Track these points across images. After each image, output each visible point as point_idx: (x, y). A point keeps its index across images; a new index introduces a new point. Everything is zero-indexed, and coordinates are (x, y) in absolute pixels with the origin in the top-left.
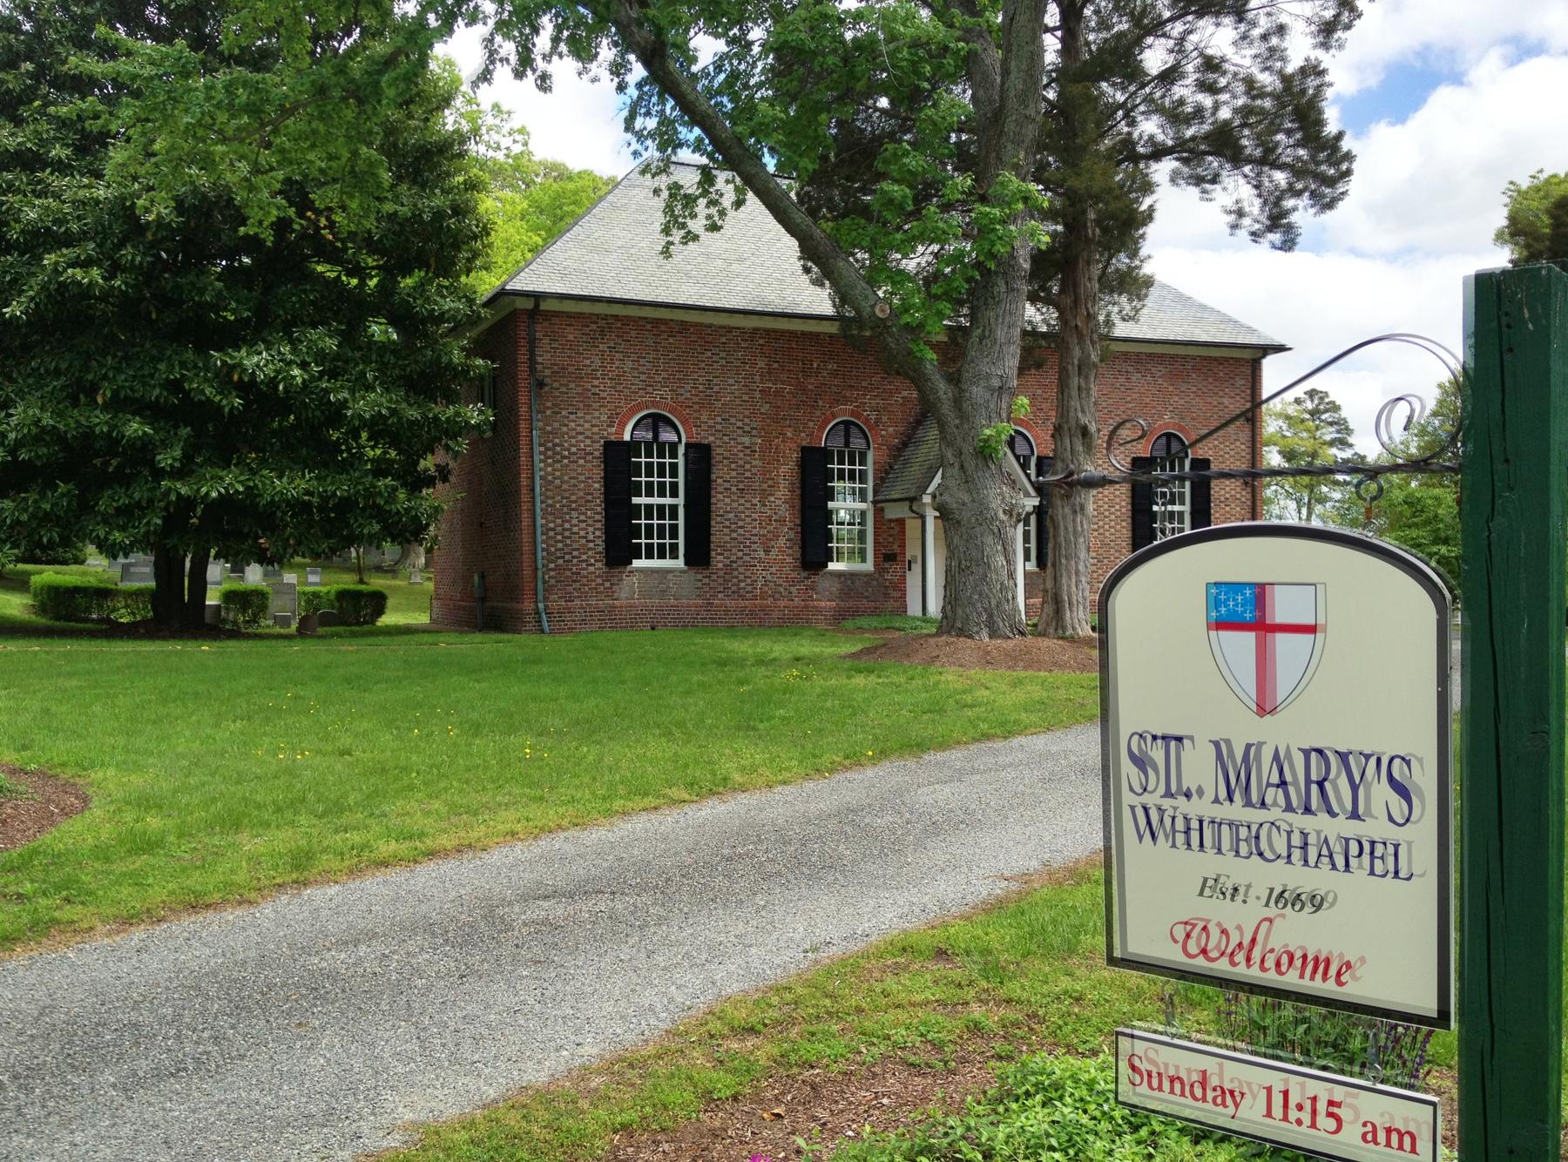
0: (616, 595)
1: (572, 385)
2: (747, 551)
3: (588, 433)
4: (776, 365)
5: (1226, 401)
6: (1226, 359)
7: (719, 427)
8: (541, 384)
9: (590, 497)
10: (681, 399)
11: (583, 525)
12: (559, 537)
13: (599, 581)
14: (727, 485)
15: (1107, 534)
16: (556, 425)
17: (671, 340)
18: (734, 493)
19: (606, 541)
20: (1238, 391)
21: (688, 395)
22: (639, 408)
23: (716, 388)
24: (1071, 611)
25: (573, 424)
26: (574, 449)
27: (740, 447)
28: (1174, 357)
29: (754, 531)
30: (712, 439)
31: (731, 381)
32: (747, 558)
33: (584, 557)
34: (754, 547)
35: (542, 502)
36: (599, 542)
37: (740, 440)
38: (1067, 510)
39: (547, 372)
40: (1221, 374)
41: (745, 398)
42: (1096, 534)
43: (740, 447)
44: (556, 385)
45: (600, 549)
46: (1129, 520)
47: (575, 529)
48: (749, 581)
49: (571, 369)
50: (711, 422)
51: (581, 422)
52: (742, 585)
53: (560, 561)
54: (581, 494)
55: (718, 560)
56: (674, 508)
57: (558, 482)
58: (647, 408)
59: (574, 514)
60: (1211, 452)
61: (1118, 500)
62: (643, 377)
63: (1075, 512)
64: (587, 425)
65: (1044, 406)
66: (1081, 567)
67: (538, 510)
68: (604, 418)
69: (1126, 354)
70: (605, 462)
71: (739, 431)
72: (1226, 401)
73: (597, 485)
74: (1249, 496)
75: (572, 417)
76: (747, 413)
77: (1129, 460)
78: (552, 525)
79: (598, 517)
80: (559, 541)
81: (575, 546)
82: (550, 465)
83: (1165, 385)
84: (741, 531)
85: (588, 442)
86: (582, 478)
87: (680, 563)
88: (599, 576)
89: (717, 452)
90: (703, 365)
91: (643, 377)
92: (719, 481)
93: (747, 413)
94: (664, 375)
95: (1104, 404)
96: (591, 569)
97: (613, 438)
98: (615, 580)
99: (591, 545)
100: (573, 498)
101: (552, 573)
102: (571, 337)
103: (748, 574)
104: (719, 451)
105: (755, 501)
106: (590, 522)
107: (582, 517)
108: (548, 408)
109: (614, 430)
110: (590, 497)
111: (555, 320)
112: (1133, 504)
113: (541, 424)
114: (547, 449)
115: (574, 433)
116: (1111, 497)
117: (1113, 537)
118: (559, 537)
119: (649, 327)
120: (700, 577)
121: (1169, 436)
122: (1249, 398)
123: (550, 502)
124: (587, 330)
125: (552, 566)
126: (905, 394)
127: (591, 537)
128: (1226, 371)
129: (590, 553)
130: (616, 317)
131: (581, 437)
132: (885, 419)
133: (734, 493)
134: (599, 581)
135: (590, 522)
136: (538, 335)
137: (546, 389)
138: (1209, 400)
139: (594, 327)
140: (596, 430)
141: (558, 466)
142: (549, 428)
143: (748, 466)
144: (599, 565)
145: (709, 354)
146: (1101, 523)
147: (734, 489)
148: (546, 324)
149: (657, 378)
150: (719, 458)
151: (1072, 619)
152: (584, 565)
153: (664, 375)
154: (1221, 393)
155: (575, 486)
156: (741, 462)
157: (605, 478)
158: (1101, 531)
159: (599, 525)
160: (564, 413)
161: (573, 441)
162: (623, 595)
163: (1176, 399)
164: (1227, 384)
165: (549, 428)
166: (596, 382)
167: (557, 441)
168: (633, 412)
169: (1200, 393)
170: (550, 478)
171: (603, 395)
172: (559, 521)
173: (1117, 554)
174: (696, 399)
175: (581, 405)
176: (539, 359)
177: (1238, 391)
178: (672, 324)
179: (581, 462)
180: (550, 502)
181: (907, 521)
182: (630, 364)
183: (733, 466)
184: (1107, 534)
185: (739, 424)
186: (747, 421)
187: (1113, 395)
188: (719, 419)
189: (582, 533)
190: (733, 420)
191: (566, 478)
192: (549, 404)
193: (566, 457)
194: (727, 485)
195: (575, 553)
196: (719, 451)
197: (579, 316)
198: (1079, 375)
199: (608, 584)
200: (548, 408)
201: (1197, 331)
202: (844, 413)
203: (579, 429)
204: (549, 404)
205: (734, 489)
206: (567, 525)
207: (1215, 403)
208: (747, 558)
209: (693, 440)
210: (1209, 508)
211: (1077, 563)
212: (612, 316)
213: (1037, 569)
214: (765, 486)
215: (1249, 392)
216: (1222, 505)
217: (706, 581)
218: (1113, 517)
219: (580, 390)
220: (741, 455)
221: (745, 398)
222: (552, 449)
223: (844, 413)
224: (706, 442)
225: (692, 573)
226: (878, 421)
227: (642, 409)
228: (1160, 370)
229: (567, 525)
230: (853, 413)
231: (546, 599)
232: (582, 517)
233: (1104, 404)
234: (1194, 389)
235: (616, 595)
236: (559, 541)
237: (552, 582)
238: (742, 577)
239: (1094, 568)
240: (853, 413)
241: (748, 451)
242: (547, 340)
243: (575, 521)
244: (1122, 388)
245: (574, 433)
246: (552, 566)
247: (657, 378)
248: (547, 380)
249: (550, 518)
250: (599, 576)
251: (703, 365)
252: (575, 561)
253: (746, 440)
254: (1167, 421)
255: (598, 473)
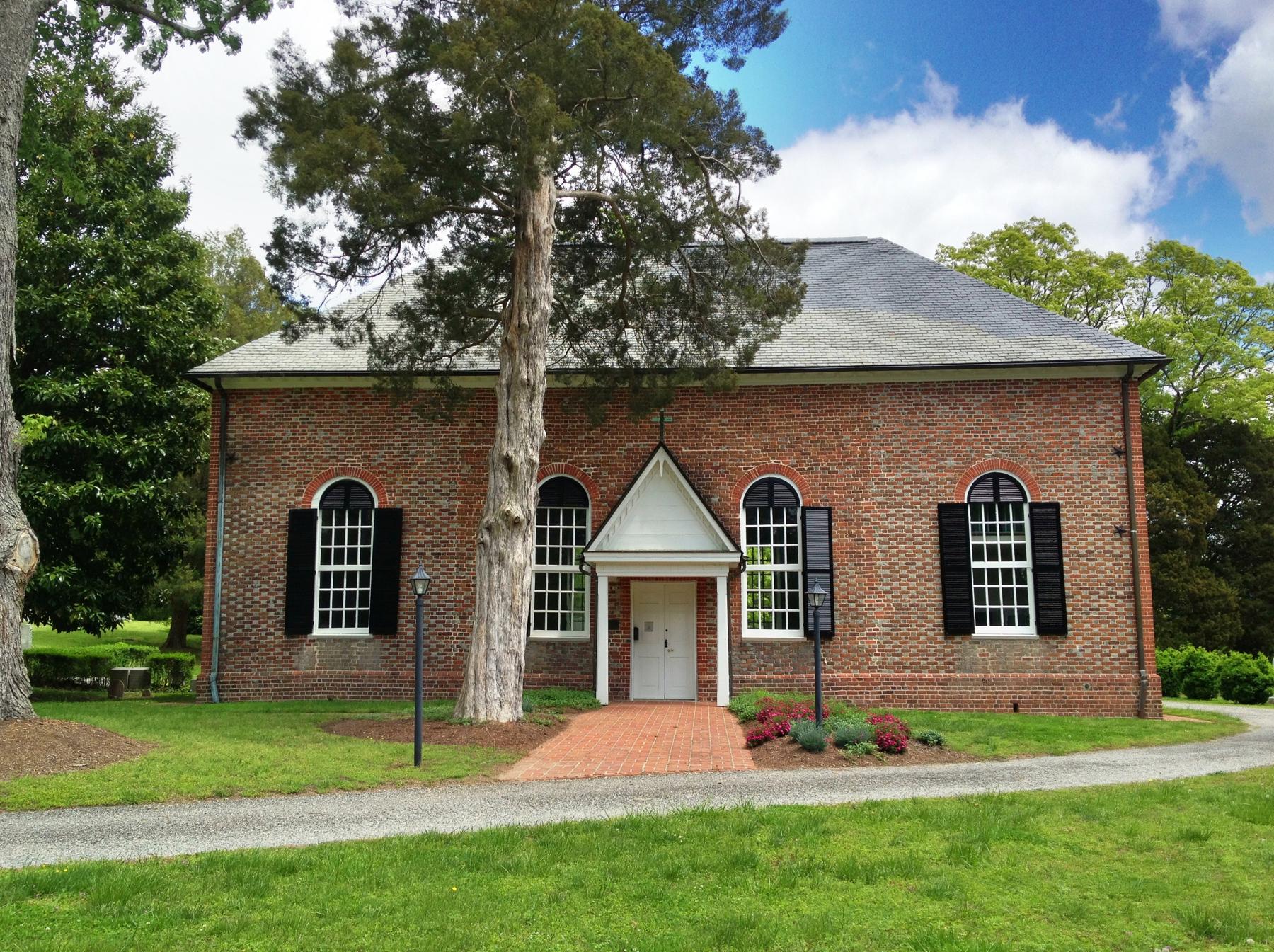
0: (294, 665)
1: (262, 458)
2: (440, 618)
3: (275, 503)
4: (479, 425)
5: (1082, 431)
6: (1081, 381)
7: (414, 491)
8: (231, 459)
9: (273, 566)
10: (375, 464)
11: (264, 594)
12: (240, 607)
13: (278, 650)
14: (421, 550)
15: (906, 597)
16: (244, 496)
17: (366, 408)
18: (428, 558)
19: (286, 610)
20: (1100, 418)
21: (382, 460)
22: (329, 476)
23: (412, 452)
24: (476, 689)
25: (260, 496)
26: (260, 520)
27: (437, 510)
28: (998, 384)
29: (449, 598)
30: (406, 503)
31: (429, 444)
32: (440, 626)
33: (264, 626)
34: (449, 613)
35: (223, 572)
36: (281, 611)
37: (437, 502)
38: (484, 561)
39: (238, 447)
40: (1073, 399)
41: (444, 459)
42: (889, 596)
43: (437, 510)
44: (246, 459)
45: (281, 617)
46: (938, 580)
47: (257, 598)
48: (441, 650)
49: (262, 442)
50: (406, 487)
51: (269, 492)
52: (434, 654)
53: (240, 631)
54: (264, 563)
55: (407, 628)
57: (242, 552)
58: (338, 475)
59: (257, 583)
60: (1061, 495)
61: (920, 556)
62: (335, 446)
63: (490, 563)
64: (274, 496)
65: (811, 450)
66: (493, 633)
67: (219, 580)
68: (292, 487)
69: (926, 384)
70: (290, 531)
71: (437, 495)
72: (1082, 431)
73: (281, 554)
74: (1126, 548)
75: (261, 488)
76: (446, 475)
77: (934, 507)
78: (233, 595)
79: (280, 586)
80: (240, 611)
81: (255, 614)
82: (235, 536)
83: (986, 416)
84: (435, 597)
85: (275, 511)
86: (266, 547)
88: (279, 646)
89: (411, 517)
90: (399, 430)
91: (335, 446)
92: (413, 546)
93: (446, 475)
94: (357, 442)
95: (896, 444)
96: (270, 638)
97: (300, 507)
98: (294, 650)
99: (272, 614)
100: (257, 567)
101: (231, 643)
102: (264, 412)
103: (441, 642)
104: (414, 515)
105: (452, 566)
106: (272, 590)
107: (265, 586)
108: (237, 481)
109: (301, 499)
110: (273, 566)
111: (249, 397)
112: (942, 560)
113: (229, 497)
114: (234, 520)
115: (261, 504)
116: (910, 552)
117: (914, 601)
118: (240, 607)
119: (343, 396)
120: (387, 645)
121: (996, 478)
122: (1119, 426)
123: (233, 571)
124: (280, 405)
125: (231, 635)
126: (631, 445)
127: (272, 606)
128: (1080, 395)
129: (270, 622)
130: (311, 390)
131: (267, 508)
132: (605, 473)
133: (428, 558)
134: (278, 650)
135: (272, 590)
136: (232, 413)
137: (237, 462)
138: (1058, 431)
139: (288, 400)
140: (283, 499)
141: (243, 536)
142: (236, 500)
143: (445, 530)
144: (279, 634)
145: (407, 418)
146: (895, 584)
147: (428, 553)
148: (240, 402)
149: (350, 446)
150: (414, 522)
151: (475, 698)
152: (263, 634)
153: (357, 442)
154: (1074, 422)
155: (258, 555)
156: (437, 526)
157: (289, 547)
158: (896, 593)
159: (281, 594)
160: (252, 484)
161: (260, 511)
162: (303, 665)
163: (1004, 432)
164: (1081, 411)
165: (236, 500)
166: (286, 453)
167: (244, 512)
168: (322, 480)
169: (1040, 423)
170: (234, 548)
171: (292, 465)
172: (241, 591)
173: (921, 621)
174: (390, 464)
175: (270, 476)
176: (232, 435)
177: (1100, 418)
178: (369, 392)
179: (267, 531)
180: (233, 571)
181: (633, 583)
182: (322, 434)
183: (428, 530)
184: (906, 597)
185: (437, 487)
186: (445, 483)
187: (909, 433)
188: (415, 483)
189: (263, 602)
190: (430, 483)
191: (250, 548)
192: (238, 477)
193: (251, 528)
194: (421, 550)
195: (255, 622)
196: (414, 515)
197: (273, 392)
198: (508, 398)
199: (287, 654)
200: (237, 481)
201: (1029, 351)
202: (557, 469)
203: (267, 499)
204: (238, 477)
205: (428, 553)
206: (248, 594)
207: (1065, 435)
208: (440, 626)
209: (385, 506)
210: (1061, 564)
211: (488, 627)
212: (307, 389)
213: (805, 639)
214: (463, 550)
215: (1118, 418)
216: (1084, 560)
217: (393, 650)
218: (913, 576)
219: (269, 462)
220: (438, 518)
221: (444, 459)
222: (239, 520)
223: (557, 469)
224: (399, 506)
225: (378, 642)
226: (596, 476)
227: (332, 477)
228: (976, 401)
229: (248, 594)
230: (567, 469)
231: (220, 668)
232: (265, 586)
233: (896, 444)
234: (1031, 419)
235: (294, 665)
236: (240, 611)
237: (230, 651)
238: (433, 646)
239: (888, 638)
240: (567, 469)
241: (445, 514)
242: (240, 417)
243: (257, 590)
244: (922, 424)
245: (261, 504)
246: (231, 635)
247: (350, 446)
248: (239, 455)
249: (231, 587)
250: (279, 646)
251: (399, 430)
252: (254, 630)
253: (444, 503)
254: (991, 459)
255: (283, 541)
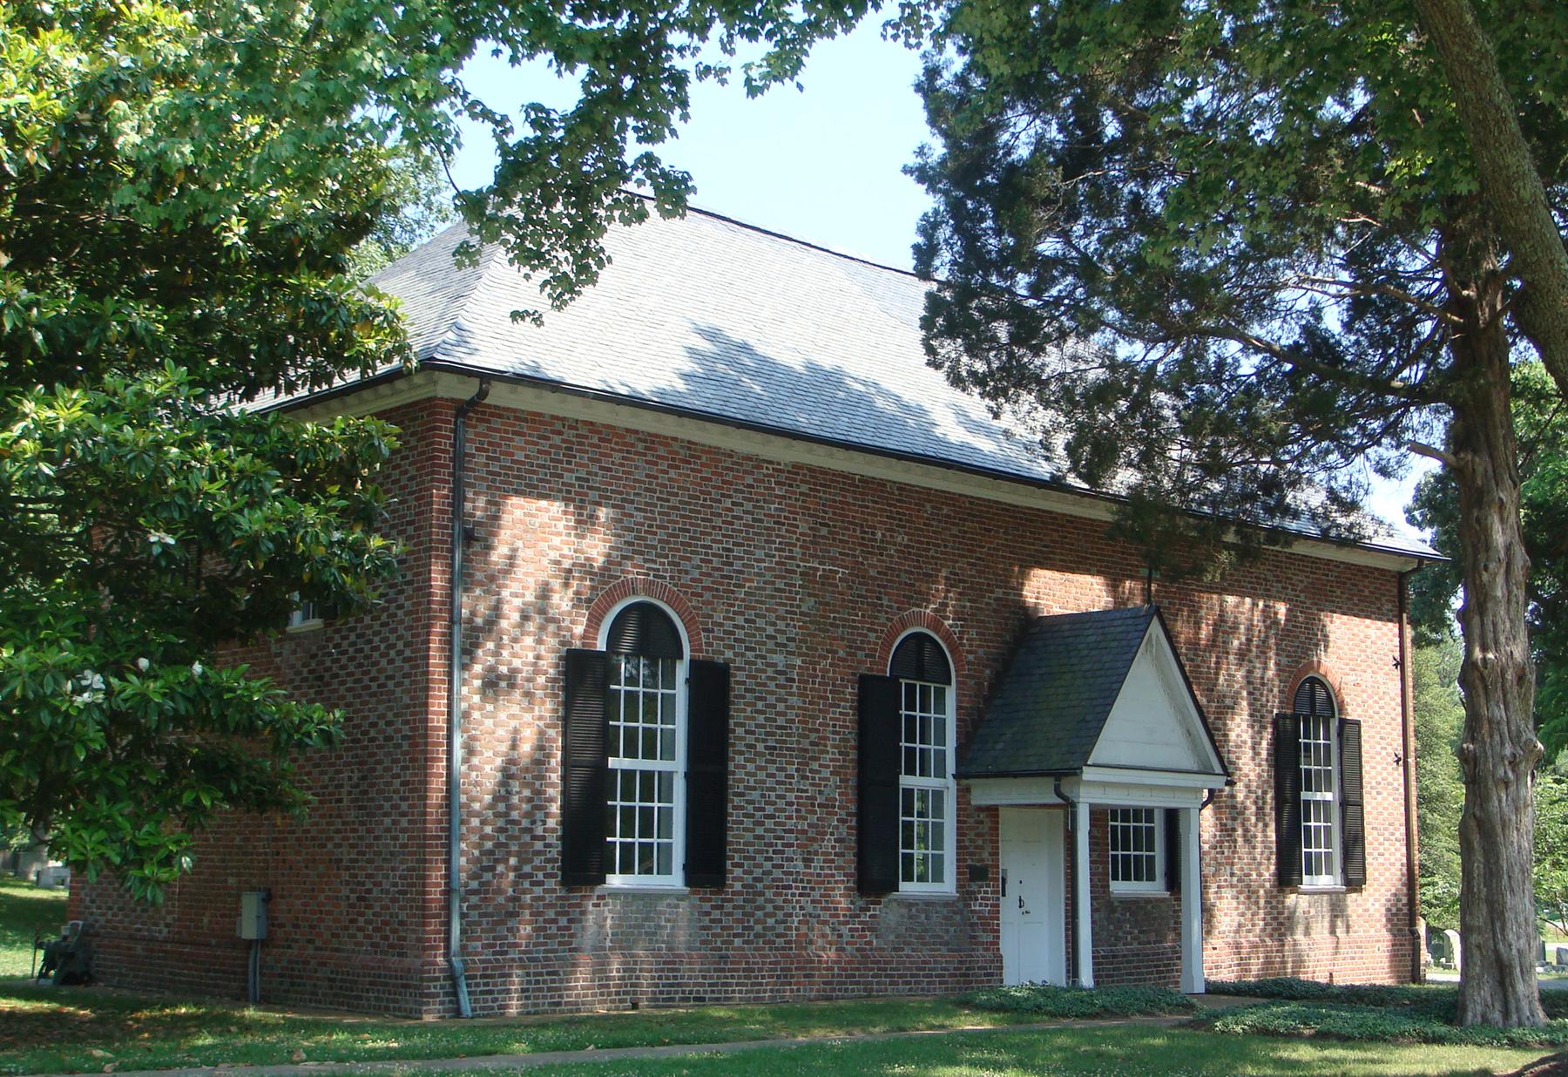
2: (777, 860)
4: (824, 531)
7: (740, 634)
10: (686, 579)
14: (750, 739)
17: (673, 474)
21: (696, 574)
23: (738, 565)
29: (790, 824)
30: (729, 654)
31: (760, 554)
32: (777, 873)
34: (789, 852)
41: (780, 584)
48: (780, 914)
52: (770, 921)
55: (736, 877)
56: (667, 778)
71: (770, 644)
84: (769, 823)
87: (675, 880)
90: (718, 522)
102: (520, 456)
103: (779, 901)
111: (497, 423)
119: (640, 447)
120: (707, 906)
129: (537, 861)
139: (557, 439)
143: (781, 707)
144: (551, 883)
145: (728, 503)
147: (760, 747)
148: (481, 428)
156: (771, 699)
174: (707, 582)
178: (676, 446)
181: (1001, 812)
185: (770, 630)
186: (781, 625)
188: (740, 620)
190: (760, 623)
194: (750, 739)
199: (563, 921)
208: (777, 873)
212: (585, 422)
213: (1167, 894)
214: (805, 744)
217: (716, 914)
220: (772, 685)
221: (780, 584)
224: (720, 659)
225: (695, 899)
238: (769, 909)
241: (782, 680)
242: (481, 459)
253: (779, 659)
